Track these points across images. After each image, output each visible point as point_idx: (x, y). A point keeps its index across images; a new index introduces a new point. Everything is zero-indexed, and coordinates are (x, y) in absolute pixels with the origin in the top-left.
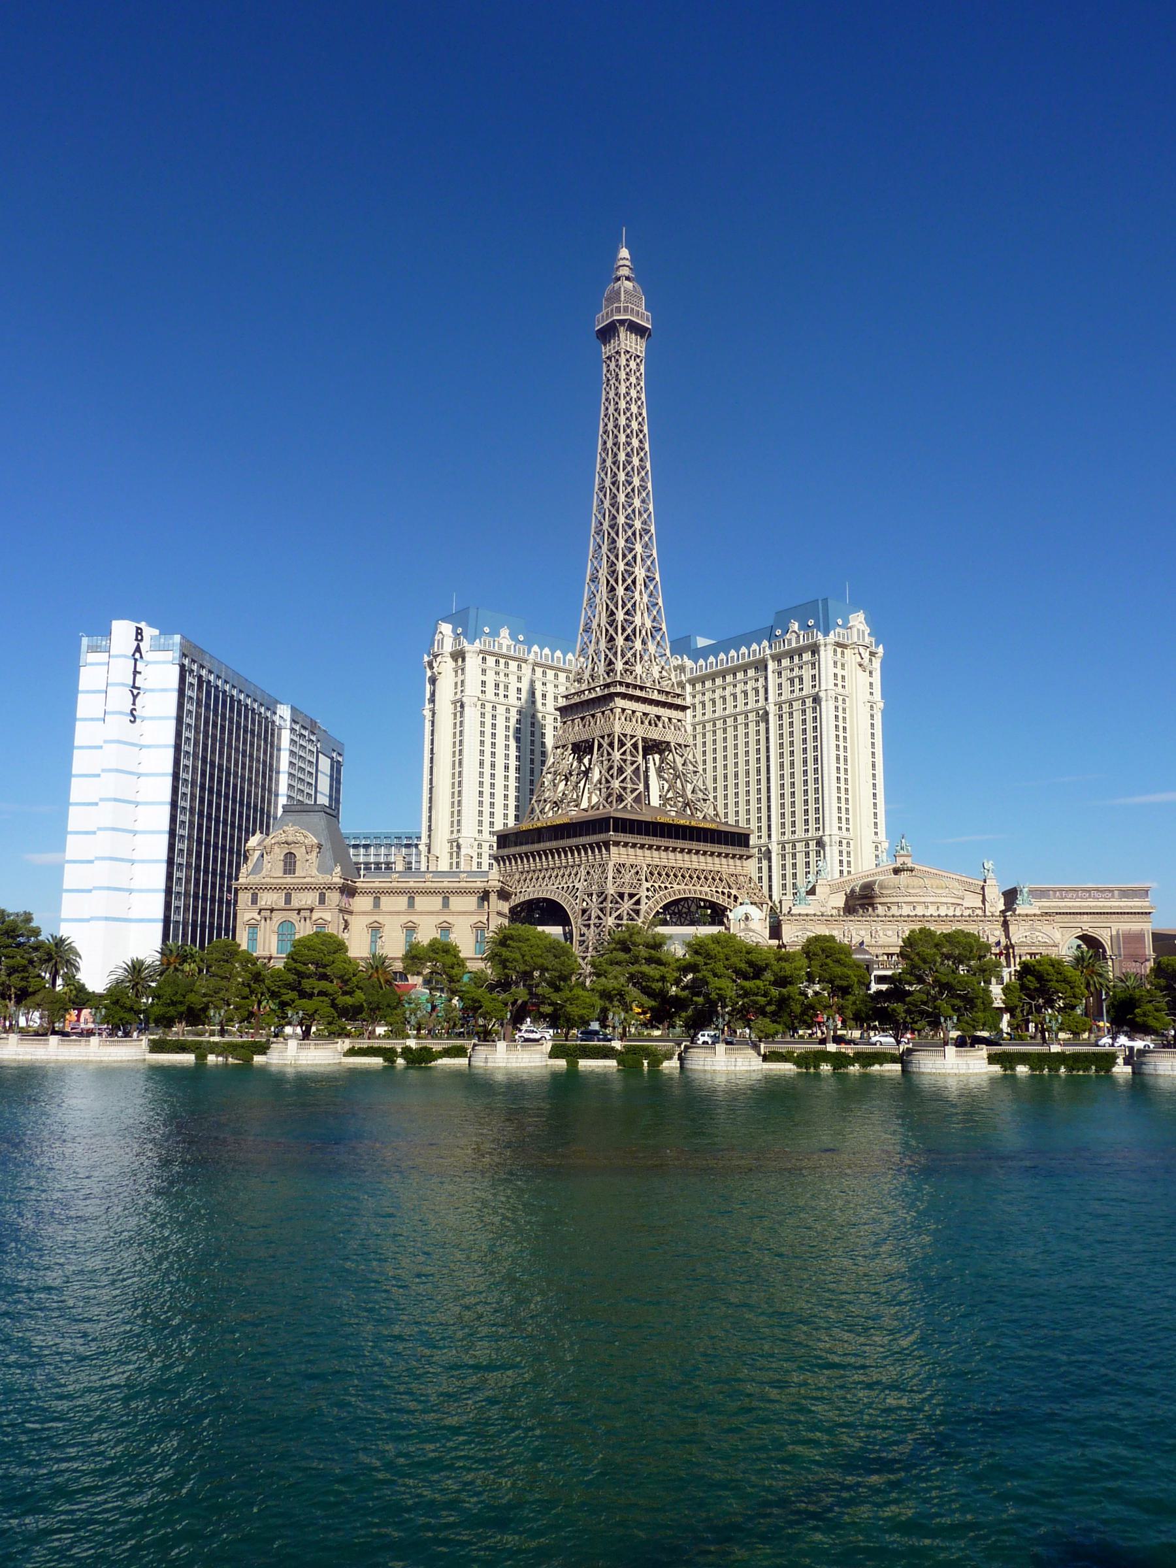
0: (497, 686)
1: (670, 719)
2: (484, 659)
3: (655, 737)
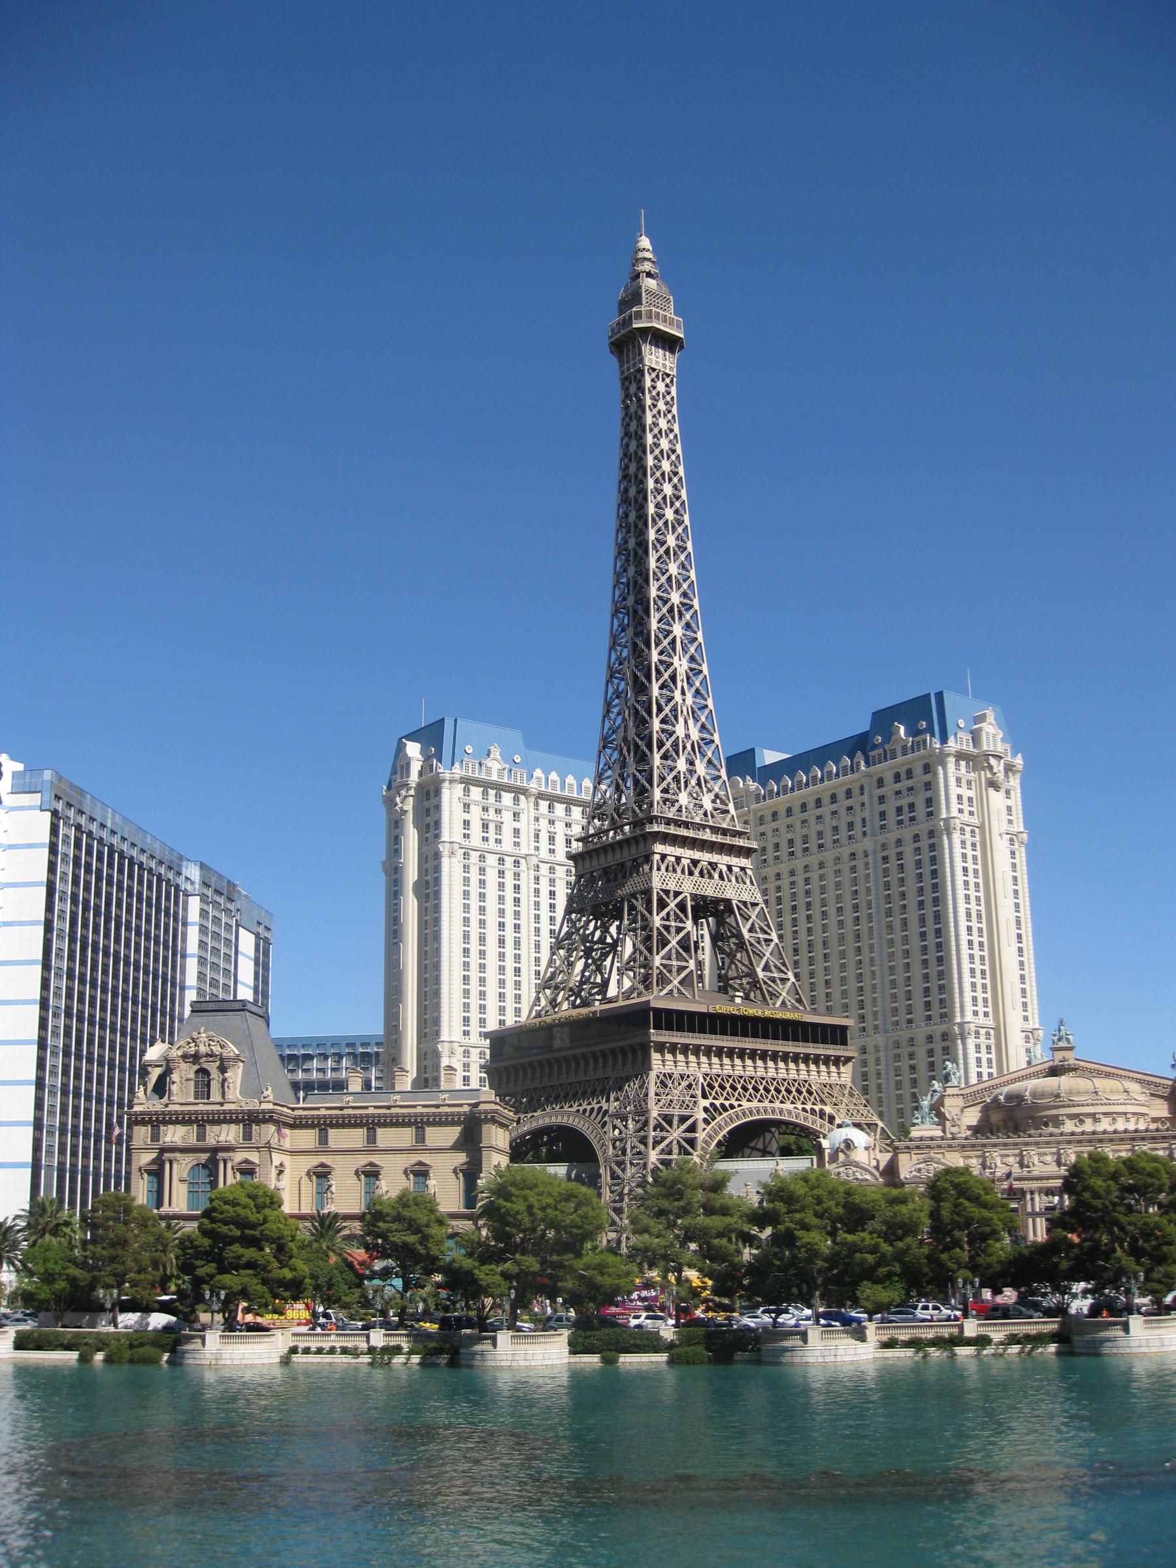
0: (485, 827)
2: (467, 791)
3: (709, 892)
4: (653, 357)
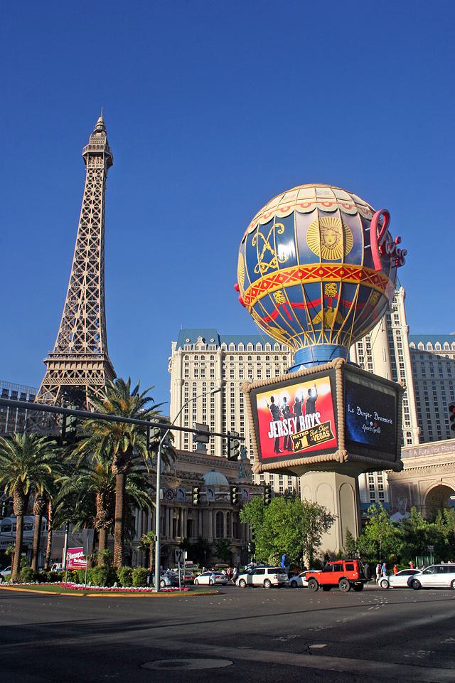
0: (196, 371)
1: (90, 372)
4: (92, 164)
